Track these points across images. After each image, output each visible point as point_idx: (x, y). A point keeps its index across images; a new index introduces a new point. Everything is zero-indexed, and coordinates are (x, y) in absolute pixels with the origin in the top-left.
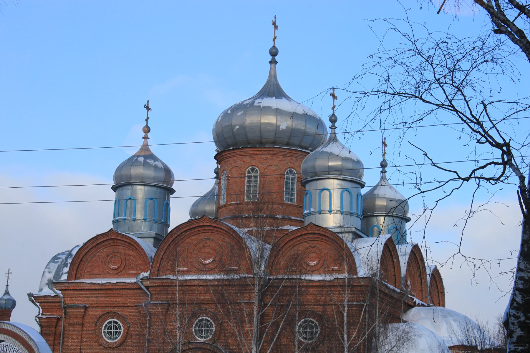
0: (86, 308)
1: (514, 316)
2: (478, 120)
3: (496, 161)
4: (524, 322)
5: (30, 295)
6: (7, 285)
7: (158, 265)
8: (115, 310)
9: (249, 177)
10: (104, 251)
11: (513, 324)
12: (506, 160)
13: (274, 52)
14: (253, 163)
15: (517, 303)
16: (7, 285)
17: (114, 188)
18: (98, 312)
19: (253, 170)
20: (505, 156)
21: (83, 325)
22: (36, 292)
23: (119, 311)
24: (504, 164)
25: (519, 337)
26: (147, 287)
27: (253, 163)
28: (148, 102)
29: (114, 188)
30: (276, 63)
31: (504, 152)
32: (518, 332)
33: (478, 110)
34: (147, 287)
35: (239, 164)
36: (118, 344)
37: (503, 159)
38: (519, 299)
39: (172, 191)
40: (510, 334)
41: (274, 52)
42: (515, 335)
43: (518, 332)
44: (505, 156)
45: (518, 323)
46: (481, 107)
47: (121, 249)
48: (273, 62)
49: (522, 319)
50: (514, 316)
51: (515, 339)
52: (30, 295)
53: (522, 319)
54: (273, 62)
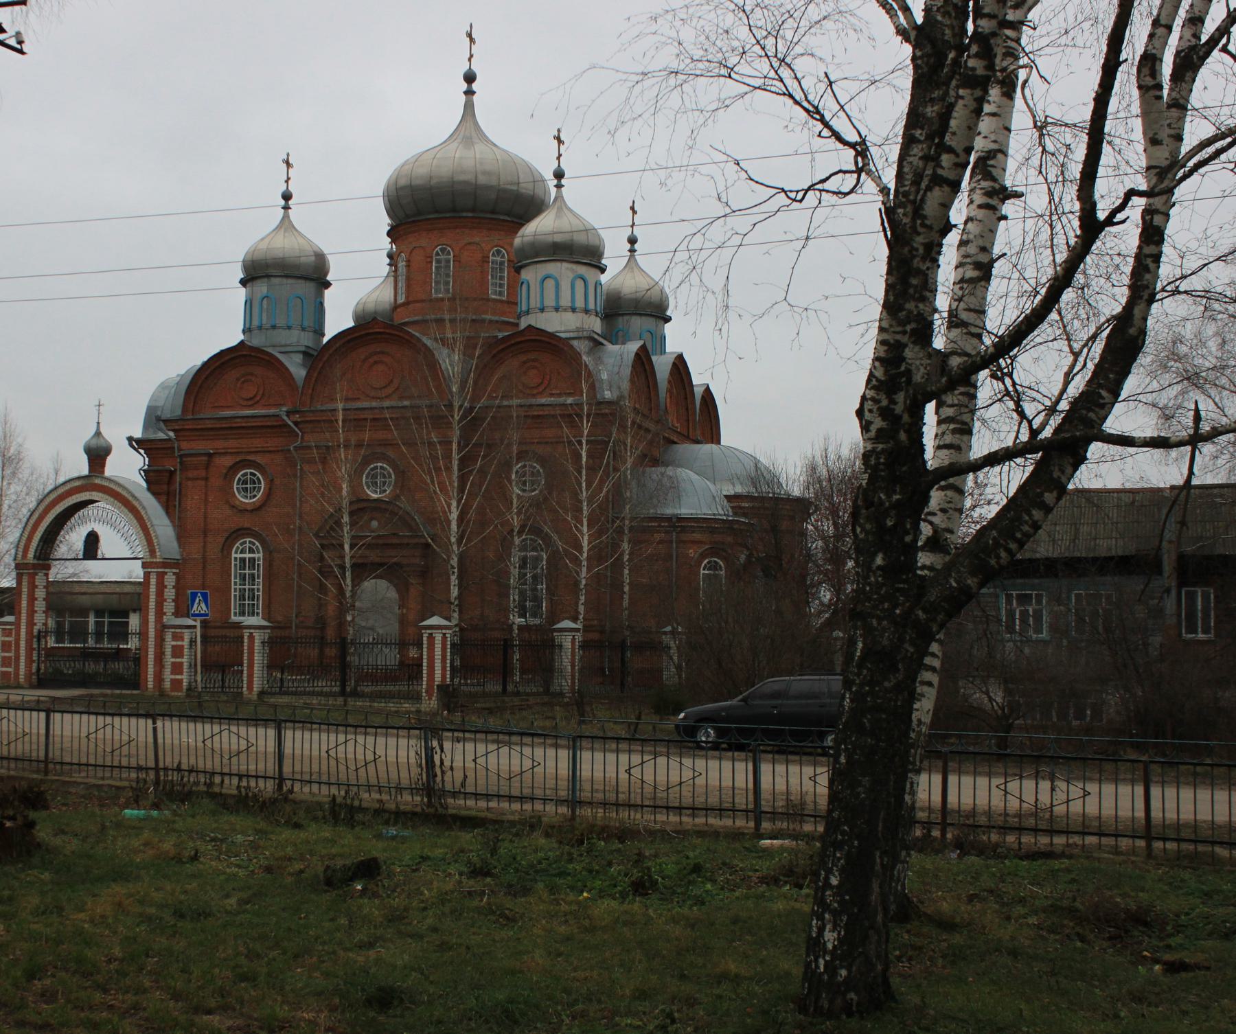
0: (210, 455)
1: (873, 399)
2: (816, 108)
3: (844, 168)
4: (887, 408)
5: (130, 439)
6: (98, 423)
7: (310, 391)
9: (438, 261)
11: (870, 411)
12: (860, 165)
13: (470, 78)
15: (877, 380)
16: (98, 423)
17: (244, 282)
18: (228, 461)
19: (443, 250)
20: (859, 159)
21: (206, 479)
22: (138, 434)
23: (258, 459)
24: (859, 171)
25: (879, 431)
28: (288, 155)
29: (244, 282)
30: (473, 93)
31: (858, 154)
32: (878, 423)
33: (815, 90)
34: (296, 423)
36: (258, 505)
37: (856, 163)
38: (879, 373)
39: (327, 285)
40: (865, 427)
41: (470, 78)
42: (874, 428)
43: (878, 423)
44: (859, 159)
45: (878, 409)
46: (823, 86)
48: (469, 93)
49: (885, 403)
50: (873, 399)
51: (873, 433)
52: (130, 439)
53: (885, 403)
54: (469, 93)
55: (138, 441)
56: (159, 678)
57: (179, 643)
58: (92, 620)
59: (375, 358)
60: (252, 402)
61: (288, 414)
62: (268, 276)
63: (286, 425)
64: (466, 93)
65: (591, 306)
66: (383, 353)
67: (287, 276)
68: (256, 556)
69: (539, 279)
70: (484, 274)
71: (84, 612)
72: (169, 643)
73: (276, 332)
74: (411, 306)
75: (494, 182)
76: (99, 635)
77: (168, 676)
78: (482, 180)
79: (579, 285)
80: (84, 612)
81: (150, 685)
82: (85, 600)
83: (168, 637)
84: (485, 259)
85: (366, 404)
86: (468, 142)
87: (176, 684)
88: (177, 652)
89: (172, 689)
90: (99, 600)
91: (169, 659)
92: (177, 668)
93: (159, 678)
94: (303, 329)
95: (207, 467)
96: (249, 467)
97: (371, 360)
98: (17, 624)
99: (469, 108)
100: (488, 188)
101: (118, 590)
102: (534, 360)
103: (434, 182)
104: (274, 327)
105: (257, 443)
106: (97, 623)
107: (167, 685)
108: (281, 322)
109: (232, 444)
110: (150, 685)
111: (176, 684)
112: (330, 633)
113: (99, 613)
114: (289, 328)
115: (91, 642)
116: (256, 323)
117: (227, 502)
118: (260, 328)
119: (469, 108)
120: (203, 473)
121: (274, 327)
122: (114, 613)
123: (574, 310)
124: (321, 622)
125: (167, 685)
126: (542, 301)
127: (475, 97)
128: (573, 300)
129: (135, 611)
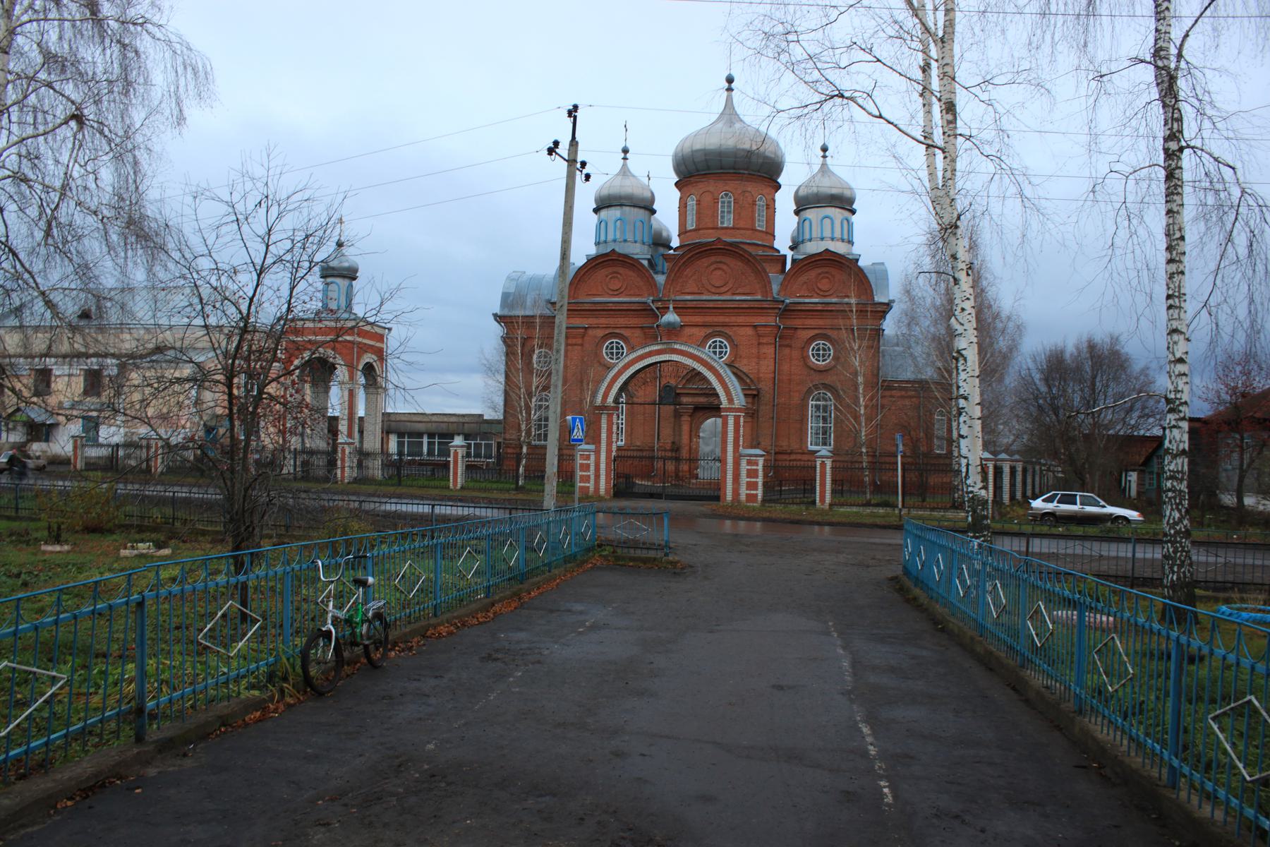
5: (495, 315)
8: (617, 331)
9: (723, 202)
10: (602, 273)
14: (727, 188)
18: (600, 333)
19: (726, 195)
21: (582, 345)
22: (498, 310)
23: (829, 333)
26: (657, 308)
27: (727, 188)
29: (596, 211)
30: (732, 90)
34: (657, 308)
35: (711, 189)
39: (653, 212)
47: (621, 270)
52: (495, 315)
55: (500, 317)
56: (736, 492)
57: (754, 467)
58: (425, 440)
59: (715, 266)
60: (617, 292)
61: (653, 301)
62: (621, 205)
63: (652, 310)
65: (645, 240)
66: (720, 262)
68: (829, 403)
69: (820, 218)
70: (753, 212)
71: (420, 435)
72: (744, 467)
73: (627, 244)
76: (430, 452)
77: (744, 492)
79: (845, 222)
80: (420, 435)
81: (729, 497)
82: (421, 427)
83: (744, 463)
84: (754, 203)
85: (704, 297)
87: (751, 498)
89: (748, 500)
90: (432, 428)
91: (744, 479)
92: (751, 486)
93: (736, 492)
94: (644, 243)
95: (583, 337)
96: (615, 337)
97: (712, 267)
98: (597, 452)
101: (446, 420)
104: (625, 241)
105: (622, 321)
106: (429, 443)
107: (743, 497)
108: (630, 237)
109: (603, 321)
110: (729, 497)
111: (751, 498)
112: (684, 453)
113: (431, 435)
114: (636, 242)
115: (425, 457)
116: (603, 238)
117: (599, 362)
118: (605, 242)
120: (579, 341)
121: (625, 241)
122: (442, 436)
123: (843, 240)
124: (676, 448)
125: (743, 497)
126: (822, 233)
128: (833, 232)
129: (459, 434)
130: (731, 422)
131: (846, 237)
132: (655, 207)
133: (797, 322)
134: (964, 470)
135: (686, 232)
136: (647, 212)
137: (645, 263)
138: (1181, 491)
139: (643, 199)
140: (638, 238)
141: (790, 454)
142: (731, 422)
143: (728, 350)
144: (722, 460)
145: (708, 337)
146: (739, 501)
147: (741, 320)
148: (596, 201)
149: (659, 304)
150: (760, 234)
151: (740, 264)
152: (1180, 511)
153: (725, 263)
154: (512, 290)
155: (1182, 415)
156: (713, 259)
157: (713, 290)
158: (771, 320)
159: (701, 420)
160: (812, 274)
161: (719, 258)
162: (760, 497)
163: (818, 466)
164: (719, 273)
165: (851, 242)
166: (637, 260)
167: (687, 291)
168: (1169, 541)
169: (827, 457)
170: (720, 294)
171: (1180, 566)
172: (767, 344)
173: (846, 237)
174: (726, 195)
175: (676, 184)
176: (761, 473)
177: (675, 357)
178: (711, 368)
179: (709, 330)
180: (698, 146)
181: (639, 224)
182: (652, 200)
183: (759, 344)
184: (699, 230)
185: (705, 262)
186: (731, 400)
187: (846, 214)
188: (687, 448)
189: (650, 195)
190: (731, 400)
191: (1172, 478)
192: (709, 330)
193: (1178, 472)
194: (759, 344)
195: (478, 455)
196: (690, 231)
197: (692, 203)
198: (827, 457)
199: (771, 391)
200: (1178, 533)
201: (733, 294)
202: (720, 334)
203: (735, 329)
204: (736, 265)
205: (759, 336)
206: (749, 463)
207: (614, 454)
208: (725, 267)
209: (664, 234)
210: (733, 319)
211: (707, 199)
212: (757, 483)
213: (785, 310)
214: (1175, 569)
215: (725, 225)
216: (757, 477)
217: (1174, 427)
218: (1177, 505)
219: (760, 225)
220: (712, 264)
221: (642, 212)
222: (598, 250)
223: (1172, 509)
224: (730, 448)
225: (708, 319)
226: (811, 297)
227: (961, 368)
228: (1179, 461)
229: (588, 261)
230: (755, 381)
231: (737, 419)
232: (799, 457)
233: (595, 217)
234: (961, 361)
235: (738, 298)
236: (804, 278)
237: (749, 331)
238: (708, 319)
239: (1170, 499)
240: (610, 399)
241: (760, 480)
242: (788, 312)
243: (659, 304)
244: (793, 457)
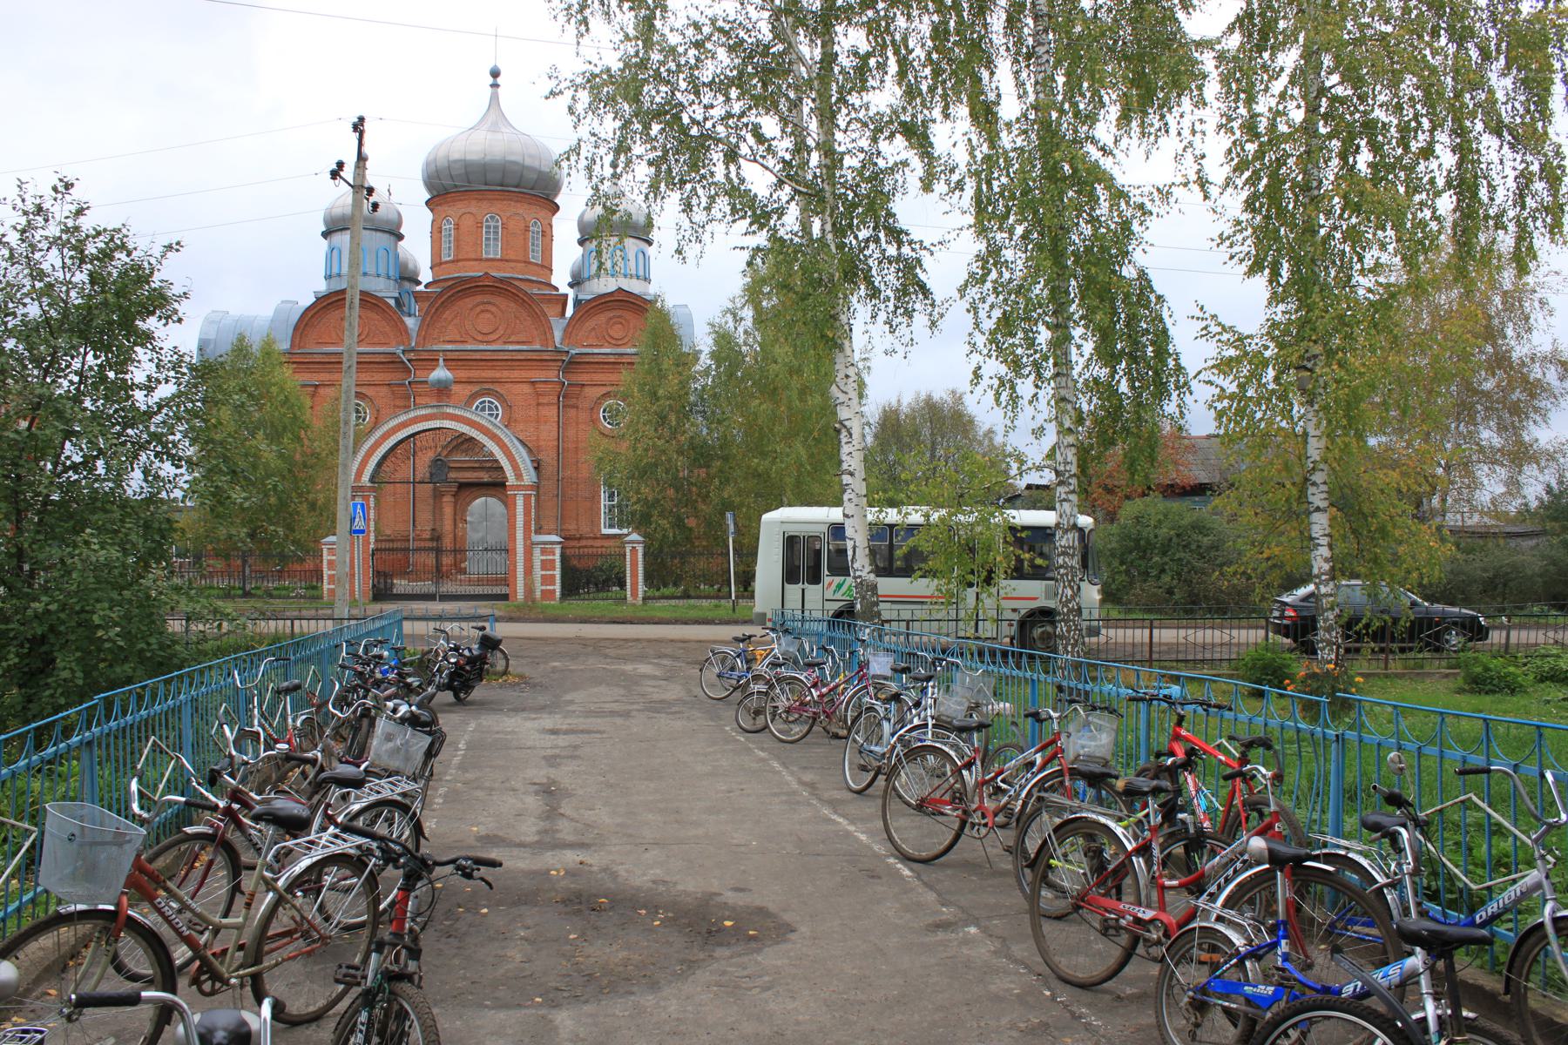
13: (495, 74)
19: (492, 218)
29: (325, 235)
35: (473, 210)
39: (400, 237)
41: (495, 74)
48: (495, 86)
54: (495, 86)
61: (404, 352)
64: (492, 86)
66: (489, 303)
67: (376, 230)
70: (526, 240)
73: (366, 278)
74: (460, 264)
75: (536, 164)
77: (539, 588)
78: (528, 162)
79: (641, 255)
81: (520, 595)
83: (537, 552)
84: (527, 229)
85: (469, 347)
86: (494, 129)
87: (548, 595)
88: (547, 565)
91: (538, 572)
92: (548, 580)
93: (529, 590)
94: (389, 278)
97: (478, 309)
99: (494, 99)
100: (531, 169)
102: (619, 317)
103: (488, 158)
107: (538, 594)
108: (371, 269)
110: (520, 595)
111: (548, 595)
112: (447, 542)
114: (378, 276)
118: (339, 275)
119: (494, 99)
123: (638, 278)
124: (436, 537)
125: (538, 594)
127: (499, 90)
130: (520, 502)
131: (641, 273)
132: (402, 231)
133: (583, 378)
134: (850, 553)
135: (441, 264)
136: (392, 238)
137: (392, 302)
138: (1072, 567)
139: (388, 222)
140: (382, 271)
141: (580, 539)
142: (520, 502)
143: (500, 412)
144: (508, 551)
145: (474, 397)
146: (534, 601)
147: (515, 374)
148: (326, 222)
149: (412, 356)
150: (536, 268)
151: (512, 305)
152: (1072, 588)
153: (494, 305)
154: (212, 336)
155: (1072, 488)
156: (479, 298)
157: (480, 337)
158: (552, 375)
159: (468, 500)
160: (603, 318)
161: (487, 298)
162: (558, 594)
163: (628, 554)
164: (488, 315)
165: (647, 279)
166: (381, 299)
167: (447, 338)
168: (1063, 620)
169: (639, 543)
170: (488, 342)
171: (1074, 646)
172: (548, 404)
173: (641, 273)
174: (492, 218)
175: (427, 203)
176: (558, 564)
177: (447, 424)
178: (493, 437)
179: (476, 388)
180: (456, 156)
181: (382, 253)
182: (399, 224)
183: (538, 404)
184: (458, 261)
185: (469, 302)
186: (519, 476)
187: (643, 245)
188: (451, 536)
189: (396, 216)
190: (519, 476)
191: (1064, 554)
192: (476, 388)
193: (1069, 547)
194: (538, 404)
195: (849, 625)
196: (446, 262)
197: (448, 227)
198: (639, 543)
199: (555, 463)
200: (1070, 611)
201: (505, 343)
202: (488, 393)
203: (507, 386)
204: (510, 307)
205: (538, 395)
206: (543, 552)
207: (372, 546)
208: (493, 309)
209: (411, 266)
210: (506, 374)
211: (468, 222)
212: (554, 576)
213: (570, 363)
214: (1069, 649)
215: (491, 256)
216: (554, 568)
217: (1065, 500)
218: (1069, 582)
219: (535, 257)
220: (478, 305)
221: (386, 237)
222: (329, 285)
223: (1064, 587)
224: (520, 535)
225: (474, 374)
226: (601, 346)
227: (844, 440)
228: (1070, 535)
229: (318, 299)
230: (534, 450)
231: (527, 498)
232: (590, 543)
233: (324, 243)
234: (844, 433)
235: (511, 347)
236: (591, 324)
237: (526, 388)
238: (474, 374)
239: (1062, 576)
240: (366, 478)
241: (557, 573)
242: (573, 364)
243: (412, 356)
244: (583, 543)
